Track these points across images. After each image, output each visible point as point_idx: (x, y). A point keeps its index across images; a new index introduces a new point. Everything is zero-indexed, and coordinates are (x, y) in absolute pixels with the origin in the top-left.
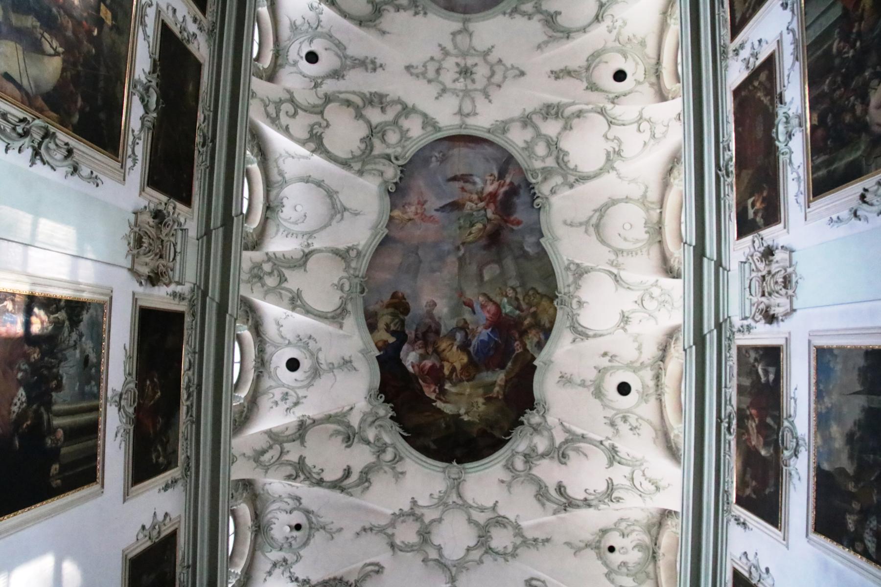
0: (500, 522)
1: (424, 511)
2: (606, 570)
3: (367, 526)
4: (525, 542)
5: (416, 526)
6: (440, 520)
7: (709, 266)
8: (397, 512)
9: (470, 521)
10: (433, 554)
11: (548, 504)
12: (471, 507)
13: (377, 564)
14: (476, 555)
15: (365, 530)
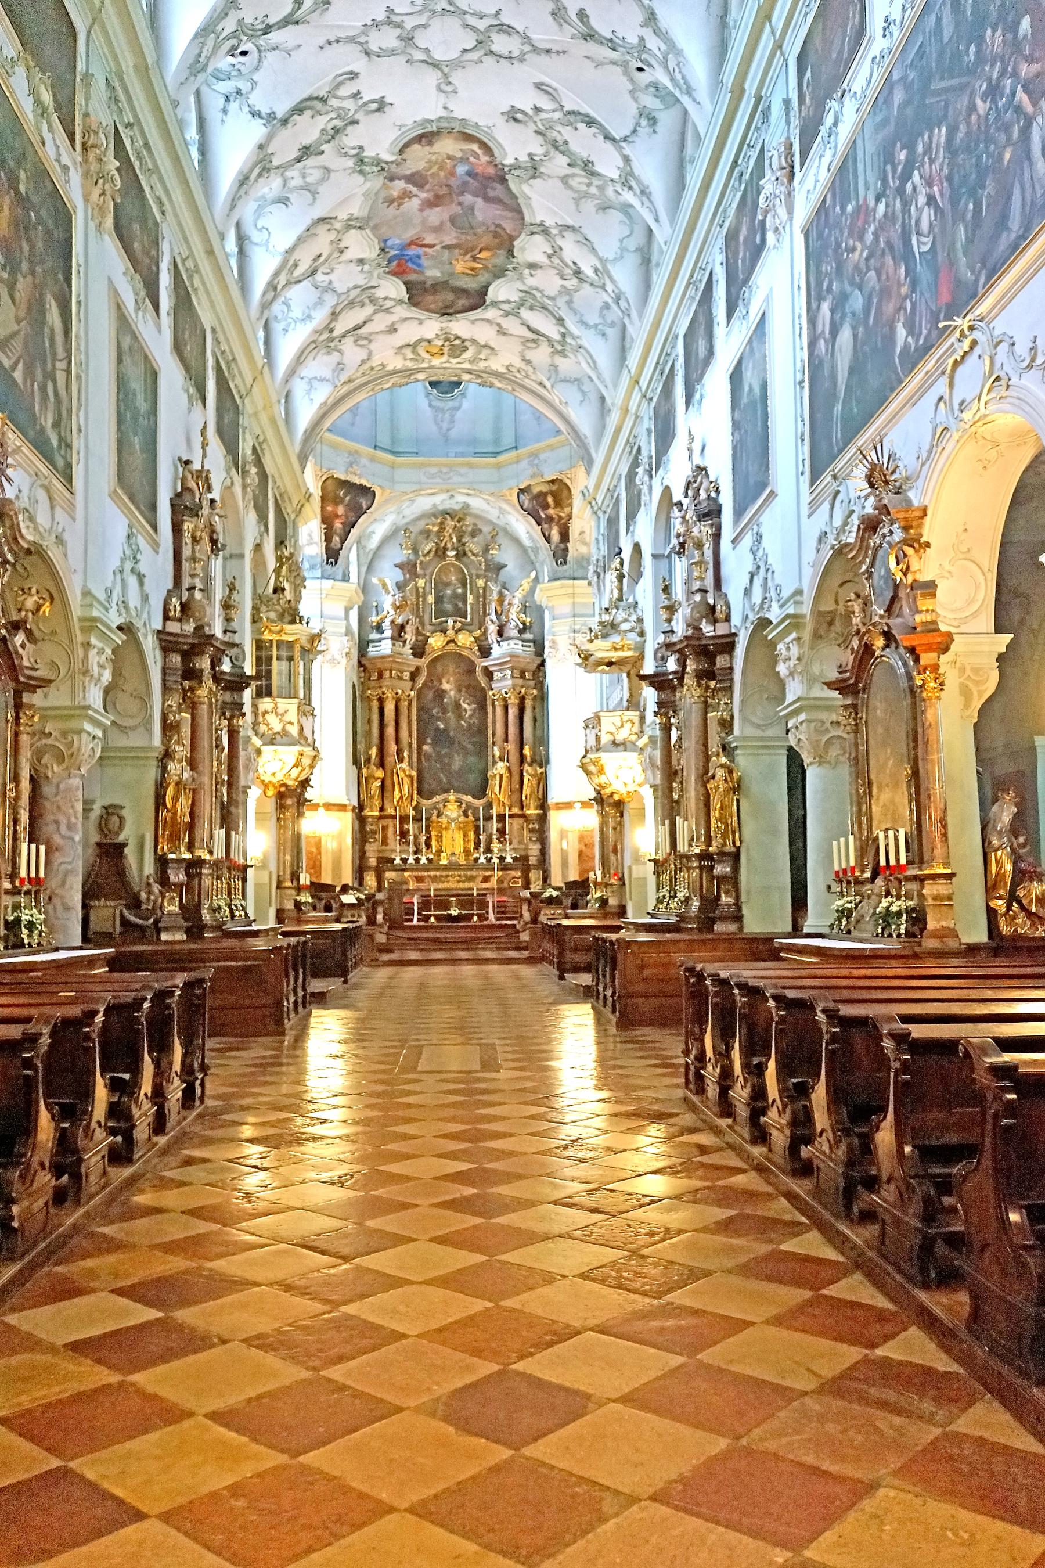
0: (506, 29)
1: (405, 18)
2: (631, 87)
3: (332, 39)
4: (535, 49)
5: (398, 31)
6: (425, 26)
7: (768, 40)
8: (369, 23)
9: (466, 26)
10: (420, 56)
11: (565, 25)
12: (465, 13)
13: (351, 73)
14: (474, 56)
15: (330, 43)
